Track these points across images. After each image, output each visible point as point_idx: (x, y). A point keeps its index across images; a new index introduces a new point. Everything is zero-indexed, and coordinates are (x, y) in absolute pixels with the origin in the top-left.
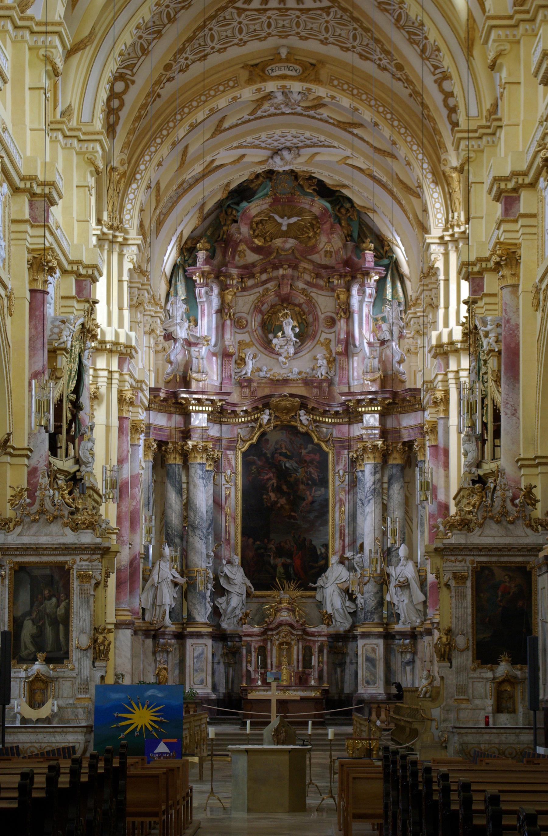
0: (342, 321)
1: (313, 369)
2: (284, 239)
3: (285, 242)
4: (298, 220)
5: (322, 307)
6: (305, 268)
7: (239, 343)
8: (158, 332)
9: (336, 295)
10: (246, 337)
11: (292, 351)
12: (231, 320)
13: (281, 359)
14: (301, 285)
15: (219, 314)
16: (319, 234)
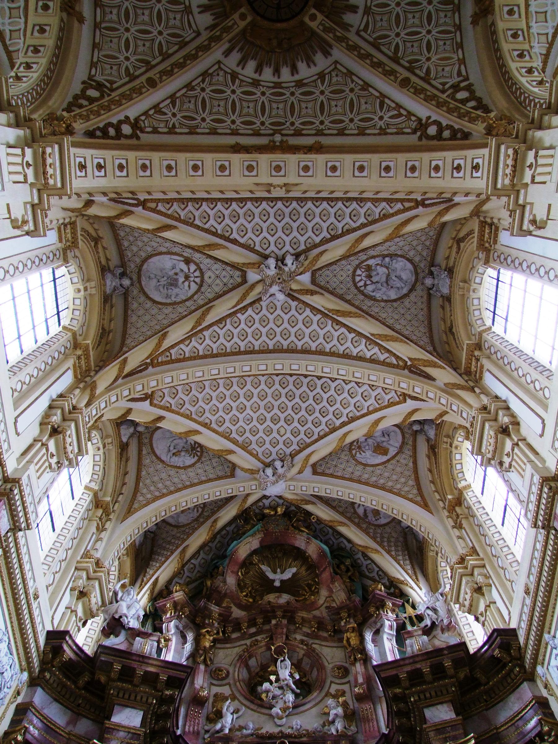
0: (358, 665)
1: (324, 725)
2: (277, 594)
3: (278, 597)
4: (294, 575)
5: (329, 659)
6: (303, 618)
7: (216, 695)
8: (93, 600)
9: (345, 642)
10: (226, 690)
11: (290, 697)
12: (206, 665)
13: (276, 710)
14: (299, 637)
15: (191, 659)
16: (318, 592)
